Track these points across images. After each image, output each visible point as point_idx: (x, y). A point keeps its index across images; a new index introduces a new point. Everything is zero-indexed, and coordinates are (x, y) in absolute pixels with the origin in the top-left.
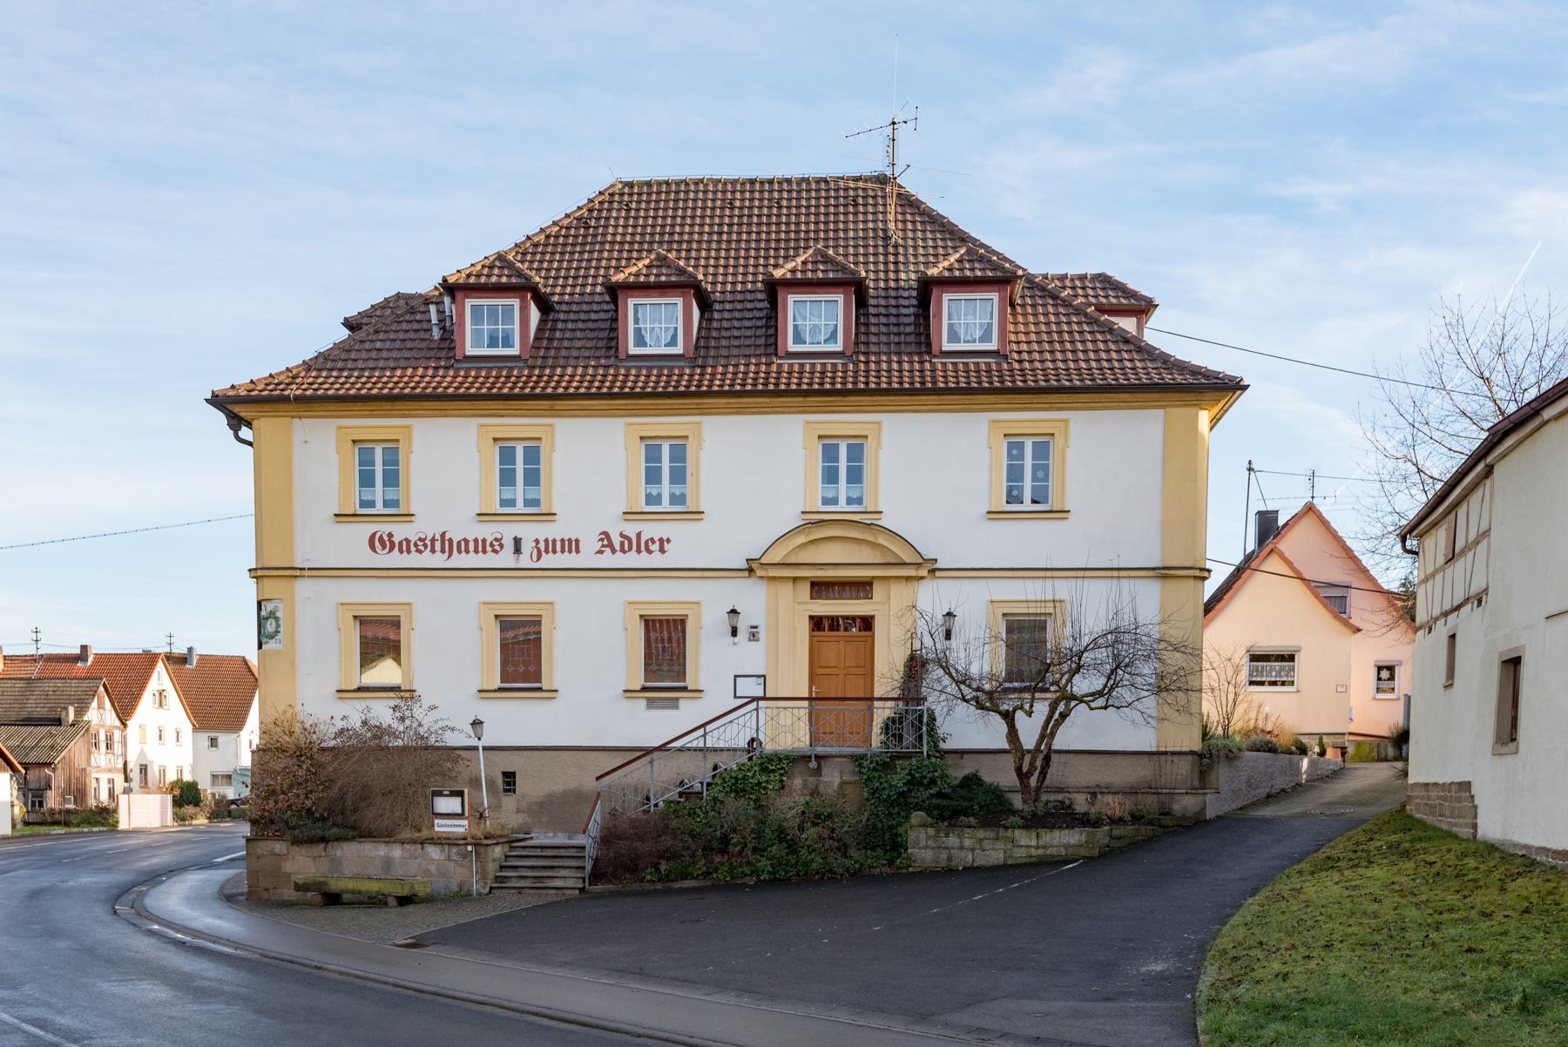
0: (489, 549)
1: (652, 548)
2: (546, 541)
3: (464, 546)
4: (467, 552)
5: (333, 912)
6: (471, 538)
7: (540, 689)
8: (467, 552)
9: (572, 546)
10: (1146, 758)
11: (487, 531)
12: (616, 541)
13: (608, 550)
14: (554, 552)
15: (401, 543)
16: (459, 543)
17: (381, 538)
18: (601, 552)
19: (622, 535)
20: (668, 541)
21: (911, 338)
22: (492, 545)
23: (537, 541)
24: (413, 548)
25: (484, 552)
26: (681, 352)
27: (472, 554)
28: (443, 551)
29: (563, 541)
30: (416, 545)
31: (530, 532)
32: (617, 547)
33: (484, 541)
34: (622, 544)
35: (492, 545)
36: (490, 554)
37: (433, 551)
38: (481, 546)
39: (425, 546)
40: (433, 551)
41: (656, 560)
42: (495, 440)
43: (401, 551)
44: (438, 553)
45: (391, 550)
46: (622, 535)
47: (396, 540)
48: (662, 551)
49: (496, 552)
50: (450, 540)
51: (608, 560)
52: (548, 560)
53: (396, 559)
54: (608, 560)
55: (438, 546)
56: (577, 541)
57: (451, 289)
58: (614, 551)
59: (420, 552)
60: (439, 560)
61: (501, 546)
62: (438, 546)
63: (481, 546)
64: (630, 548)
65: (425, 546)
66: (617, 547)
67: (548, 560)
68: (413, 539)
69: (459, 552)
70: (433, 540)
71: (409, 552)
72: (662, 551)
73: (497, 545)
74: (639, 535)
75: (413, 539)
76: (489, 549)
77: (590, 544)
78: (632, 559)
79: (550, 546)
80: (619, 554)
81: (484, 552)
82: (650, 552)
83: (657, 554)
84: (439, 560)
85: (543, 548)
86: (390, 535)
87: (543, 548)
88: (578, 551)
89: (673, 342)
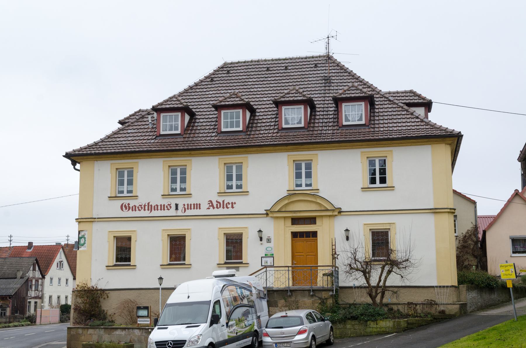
0: (166, 208)
1: (228, 206)
2: (188, 205)
3: (156, 208)
4: (158, 210)
6: (159, 205)
7: (184, 264)
8: (158, 210)
9: (198, 206)
11: (165, 202)
12: (215, 204)
13: (211, 208)
17: (125, 205)
18: (209, 208)
19: (217, 202)
20: (235, 203)
22: (167, 207)
23: (184, 205)
24: (137, 209)
26: (241, 129)
27: (159, 210)
28: (148, 210)
31: (181, 202)
32: (215, 206)
34: (217, 205)
35: (167, 207)
36: (166, 210)
37: (145, 210)
39: (142, 208)
40: (145, 210)
41: (230, 211)
43: (133, 210)
45: (129, 210)
46: (217, 202)
47: (131, 206)
48: (233, 207)
49: (168, 209)
50: (151, 206)
51: (212, 211)
52: (189, 212)
53: (131, 213)
54: (212, 211)
55: (146, 207)
56: (200, 204)
57: (158, 109)
58: (214, 208)
59: (140, 210)
60: (146, 213)
61: (171, 207)
62: (146, 207)
64: (220, 207)
65: (142, 208)
66: (215, 206)
67: (189, 212)
68: (137, 205)
69: (155, 210)
70: (145, 206)
71: (135, 210)
73: (169, 207)
74: (223, 201)
75: (137, 205)
77: (205, 205)
78: (221, 211)
79: (189, 207)
80: (216, 209)
81: (164, 209)
82: (228, 208)
83: (231, 209)
84: (146, 213)
85: (186, 208)
86: (129, 204)
87: (186, 208)
88: (200, 208)
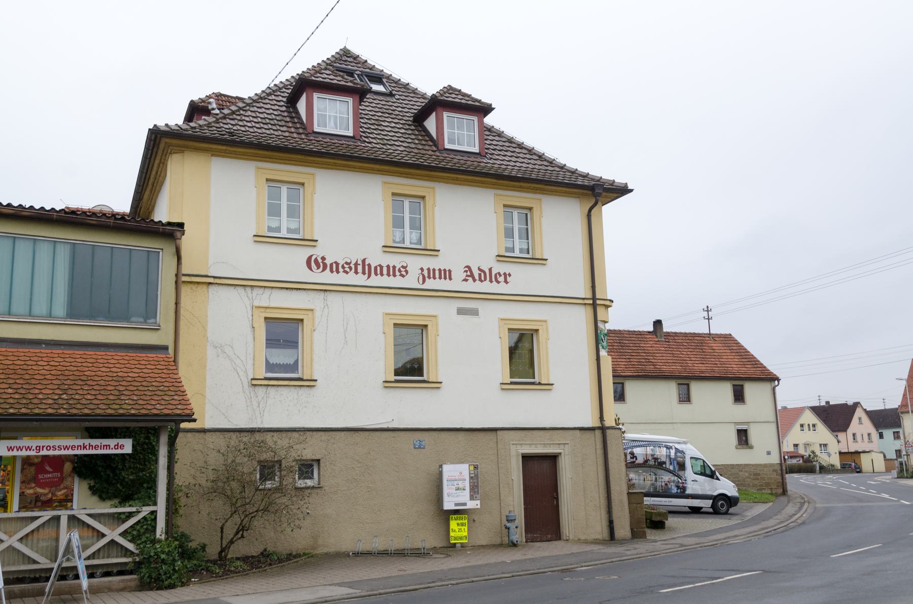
0: (397, 273)
1: (500, 279)
2: (429, 269)
3: (379, 270)
4: (382, 274)
5: (515, 549)
7: (424, 382)
8: (382, 274)
9: (446, 274)
10: (578, 432)
11: (396, 261)
12: (476, 273)
13: (470, 279)
14: (434, 278)
15: (331, 265)
16: (376, 268)
17: (316, 260)
18: (466, 280)
19: (479, 269)
20: (510, 275)
21: (284, 109)
22: (400, 271)
23: (422, 269)
24: (341, 270)
25: (394, 275)
26: (478, 151)
27: (385, 276)
28: (364, 273)
29: (440, 270)
30: (343, 267)
31: (415, 264)
32: (477, 277)
33: (394, 267)
34: (480, 275)
35: (400, 271)
36: (398, 277)
37: (356, 272)
38: (392, 271)
39: (350, 268)
41: (501, 288)
42: (267, 180)
43: (332, 271)
44: (360, 275)
45: (324, 270)
46: (479, 269)
47: (328, 262)
48: (506, 282)
49: (403, 276)
50: (369, 265)
51: (471, 286)
52: (430, 284)
53: (327, 277)
54: (471, 286)
55: (360, 268)
56: (450, 271)
58: (474, 280)
59: (347, 273)
60: (360, 279)
61: (407, 272)
62: (360, 268)
63: (392, 271)
64: (485, 279)
65: (350, 268)
66: (477, 277)
67: (430, 284)
68: (341, 263)
69: (376, 274)
70: (356, 264)
72: (506, 282)
74: (490, 270)
75: (341, 263)
76: (397, 273)
77: (459, 274)
78: (486, 287)
79: (431, 274)
80: (478, 282)
81: (394, 275)
83: (503, 283)
84: (360, 279)
85: (426, 275)
86: (323, 258)
87: (426, 275)
88: (450, 279)
89: (451, 141)
